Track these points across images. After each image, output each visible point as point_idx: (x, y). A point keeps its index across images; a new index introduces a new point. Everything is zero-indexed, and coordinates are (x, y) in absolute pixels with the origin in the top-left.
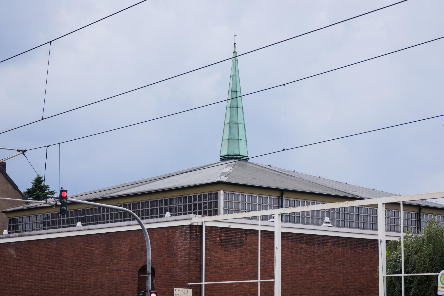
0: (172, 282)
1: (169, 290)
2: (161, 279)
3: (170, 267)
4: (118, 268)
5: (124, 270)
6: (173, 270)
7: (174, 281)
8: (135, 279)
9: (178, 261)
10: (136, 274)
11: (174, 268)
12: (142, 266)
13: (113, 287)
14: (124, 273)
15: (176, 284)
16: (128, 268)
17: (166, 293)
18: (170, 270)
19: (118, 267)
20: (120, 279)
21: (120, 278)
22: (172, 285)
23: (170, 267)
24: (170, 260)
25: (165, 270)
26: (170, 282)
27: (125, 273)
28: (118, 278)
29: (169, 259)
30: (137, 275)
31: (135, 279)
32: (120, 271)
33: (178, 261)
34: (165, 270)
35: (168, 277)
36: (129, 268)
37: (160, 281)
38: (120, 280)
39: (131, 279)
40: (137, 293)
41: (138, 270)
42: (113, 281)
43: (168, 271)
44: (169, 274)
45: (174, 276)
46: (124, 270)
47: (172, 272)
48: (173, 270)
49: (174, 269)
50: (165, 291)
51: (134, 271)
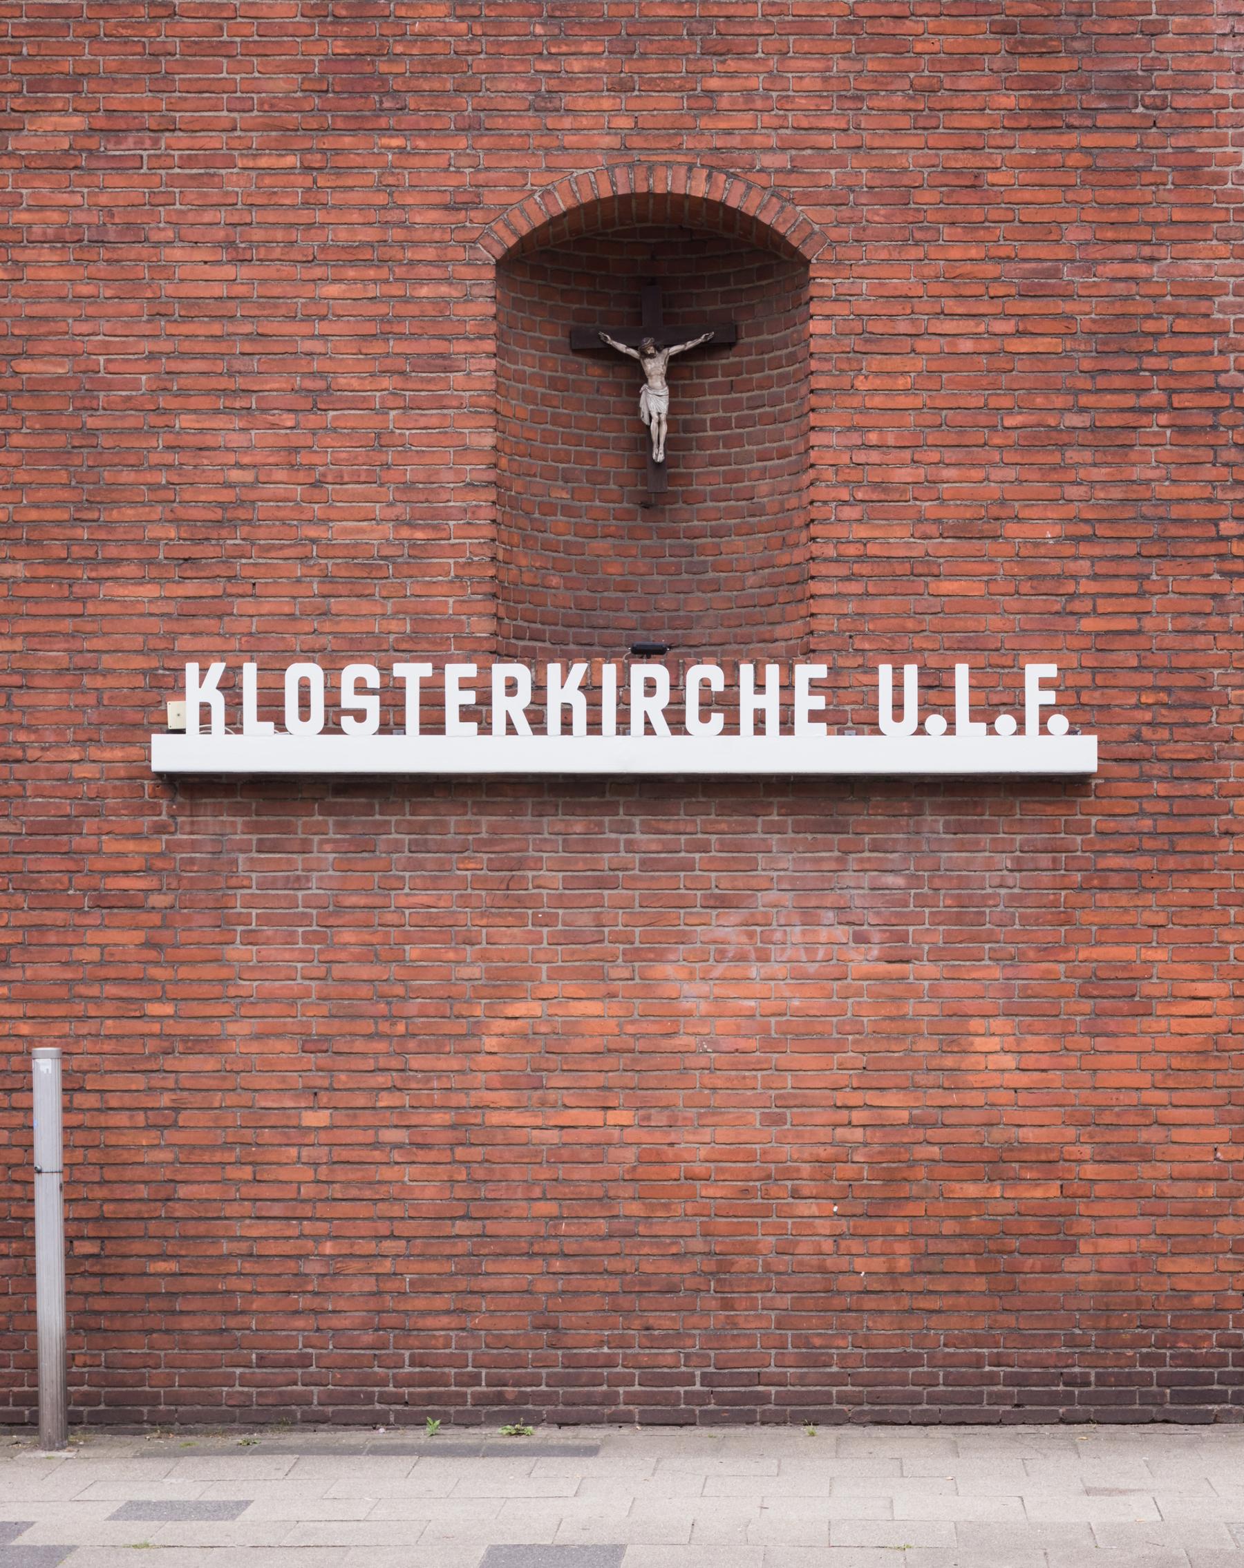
0: (1129, 400)
1: (1073, 492)
2: (922, 363)
3: (1073, 234)
4: (109, 210)
5: (230, 244)
6: (1142, 270)
7: (1157, 397)
8: (439, 346)
9: (1220, 179)
10: (468, 299)
11: (1147, 251)
12: (562, 204)
13: (15, 440)
14: (229, 271)
15: (1183, 430)
16: (304, 216)
17: (1011, 529)
18: (1088, 271)
19: (103, 200)
20: (165, 346)
21: (147, 329)
22: (1132, 437)
23: (1073, 234)
24: (1075, 159)
25: (991, 269)
26: (1084, 400)
27: (244, 272)
28: (105, 326)
29: (1073, 139)
30: (473, 309)
31: (439, 346)
32: (145, 251)
33: (1220, 179)
34: (991, 269)
35: (1042, 344)
36: (319, 216)
37: (901, 382)
38: (152, 356)
39: (377, 348)
40: (488, 513)
41: (488, 253)
42: (24, 366)
43: (1056, 273)
44: (1070, 317)
45: (1157, 335)
46: (230, 244)
47: (1120, 288)
48: (1142, 270)
49: (1153, 259)
50: (1003, 502)
51: (430, 253)
